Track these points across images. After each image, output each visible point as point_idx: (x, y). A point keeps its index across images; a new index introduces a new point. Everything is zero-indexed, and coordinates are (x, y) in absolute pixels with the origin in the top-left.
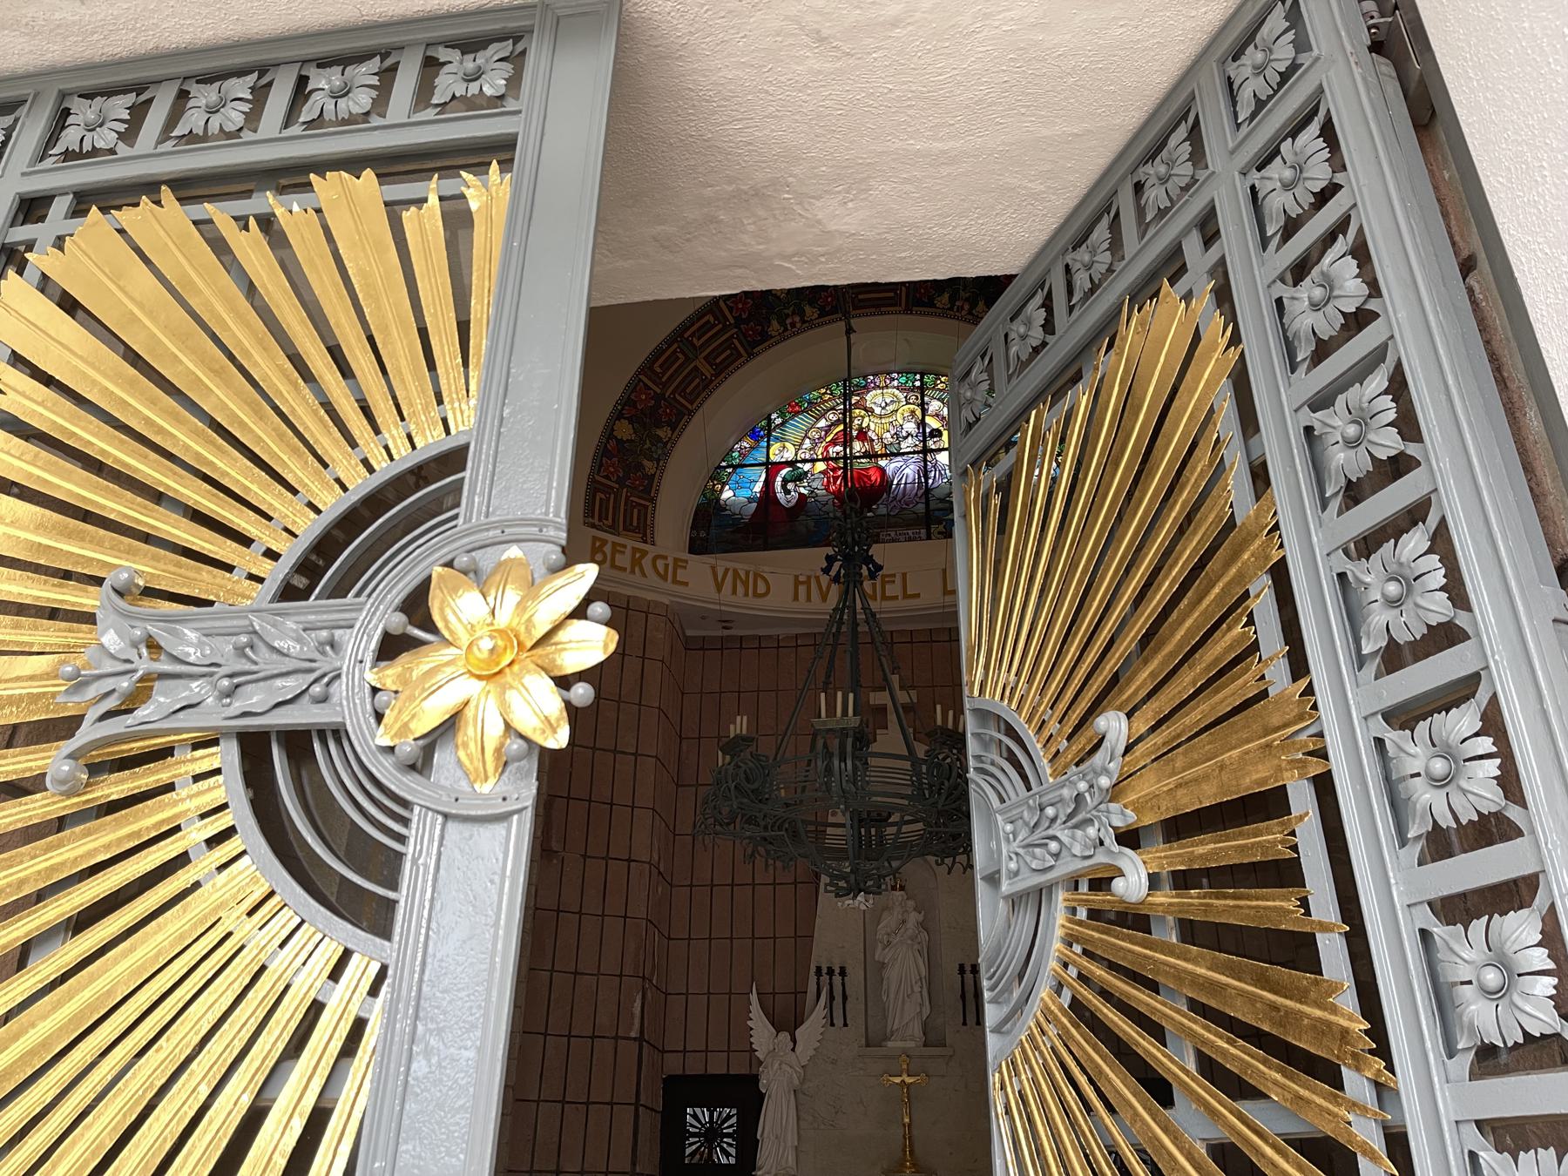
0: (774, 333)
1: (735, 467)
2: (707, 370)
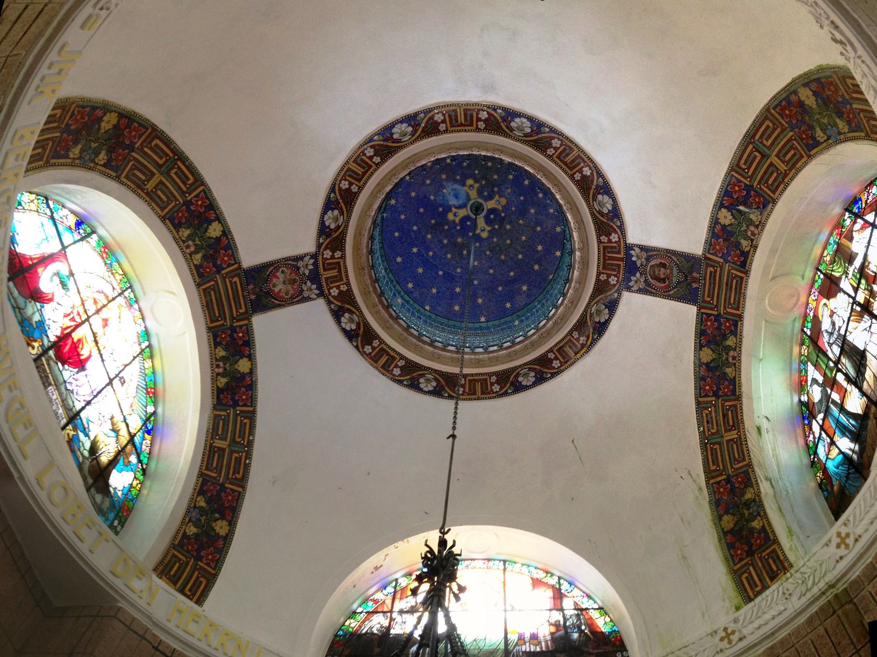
0: (180, 233)
2: (150, 186)
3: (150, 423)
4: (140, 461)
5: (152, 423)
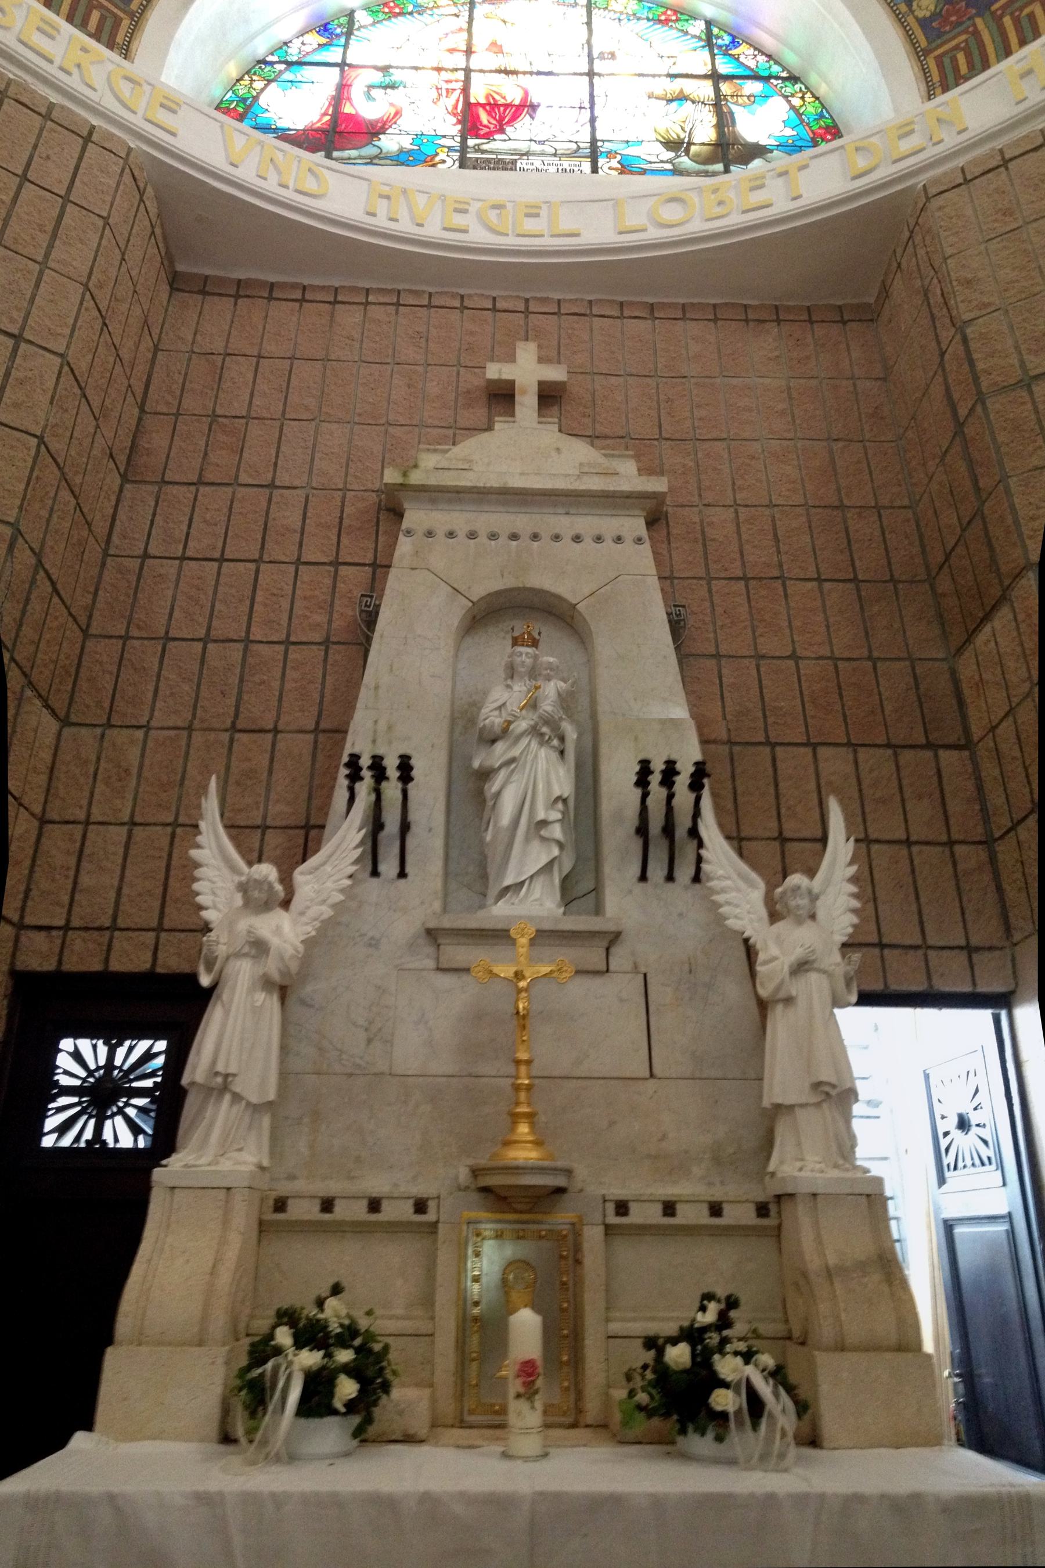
1: (289, 64)
3: (718, 37)
4: (766, 79)
5: (722, 33)
